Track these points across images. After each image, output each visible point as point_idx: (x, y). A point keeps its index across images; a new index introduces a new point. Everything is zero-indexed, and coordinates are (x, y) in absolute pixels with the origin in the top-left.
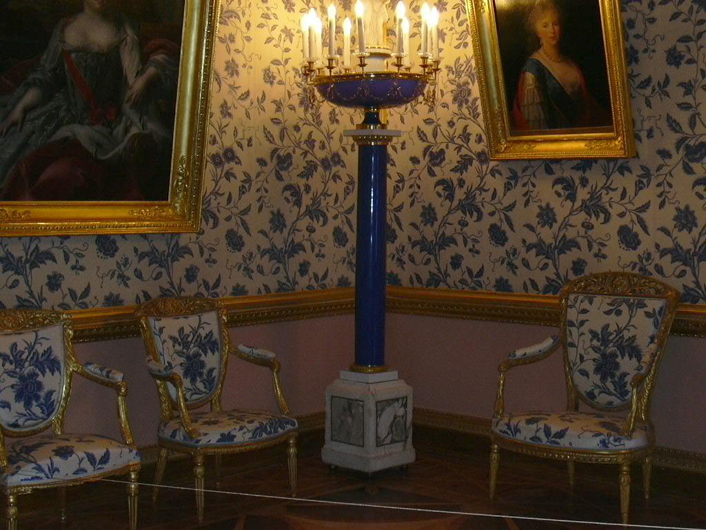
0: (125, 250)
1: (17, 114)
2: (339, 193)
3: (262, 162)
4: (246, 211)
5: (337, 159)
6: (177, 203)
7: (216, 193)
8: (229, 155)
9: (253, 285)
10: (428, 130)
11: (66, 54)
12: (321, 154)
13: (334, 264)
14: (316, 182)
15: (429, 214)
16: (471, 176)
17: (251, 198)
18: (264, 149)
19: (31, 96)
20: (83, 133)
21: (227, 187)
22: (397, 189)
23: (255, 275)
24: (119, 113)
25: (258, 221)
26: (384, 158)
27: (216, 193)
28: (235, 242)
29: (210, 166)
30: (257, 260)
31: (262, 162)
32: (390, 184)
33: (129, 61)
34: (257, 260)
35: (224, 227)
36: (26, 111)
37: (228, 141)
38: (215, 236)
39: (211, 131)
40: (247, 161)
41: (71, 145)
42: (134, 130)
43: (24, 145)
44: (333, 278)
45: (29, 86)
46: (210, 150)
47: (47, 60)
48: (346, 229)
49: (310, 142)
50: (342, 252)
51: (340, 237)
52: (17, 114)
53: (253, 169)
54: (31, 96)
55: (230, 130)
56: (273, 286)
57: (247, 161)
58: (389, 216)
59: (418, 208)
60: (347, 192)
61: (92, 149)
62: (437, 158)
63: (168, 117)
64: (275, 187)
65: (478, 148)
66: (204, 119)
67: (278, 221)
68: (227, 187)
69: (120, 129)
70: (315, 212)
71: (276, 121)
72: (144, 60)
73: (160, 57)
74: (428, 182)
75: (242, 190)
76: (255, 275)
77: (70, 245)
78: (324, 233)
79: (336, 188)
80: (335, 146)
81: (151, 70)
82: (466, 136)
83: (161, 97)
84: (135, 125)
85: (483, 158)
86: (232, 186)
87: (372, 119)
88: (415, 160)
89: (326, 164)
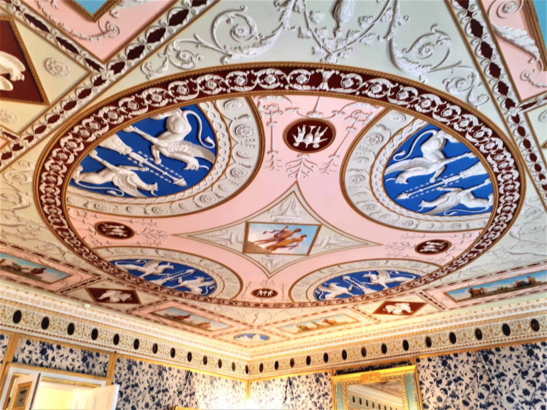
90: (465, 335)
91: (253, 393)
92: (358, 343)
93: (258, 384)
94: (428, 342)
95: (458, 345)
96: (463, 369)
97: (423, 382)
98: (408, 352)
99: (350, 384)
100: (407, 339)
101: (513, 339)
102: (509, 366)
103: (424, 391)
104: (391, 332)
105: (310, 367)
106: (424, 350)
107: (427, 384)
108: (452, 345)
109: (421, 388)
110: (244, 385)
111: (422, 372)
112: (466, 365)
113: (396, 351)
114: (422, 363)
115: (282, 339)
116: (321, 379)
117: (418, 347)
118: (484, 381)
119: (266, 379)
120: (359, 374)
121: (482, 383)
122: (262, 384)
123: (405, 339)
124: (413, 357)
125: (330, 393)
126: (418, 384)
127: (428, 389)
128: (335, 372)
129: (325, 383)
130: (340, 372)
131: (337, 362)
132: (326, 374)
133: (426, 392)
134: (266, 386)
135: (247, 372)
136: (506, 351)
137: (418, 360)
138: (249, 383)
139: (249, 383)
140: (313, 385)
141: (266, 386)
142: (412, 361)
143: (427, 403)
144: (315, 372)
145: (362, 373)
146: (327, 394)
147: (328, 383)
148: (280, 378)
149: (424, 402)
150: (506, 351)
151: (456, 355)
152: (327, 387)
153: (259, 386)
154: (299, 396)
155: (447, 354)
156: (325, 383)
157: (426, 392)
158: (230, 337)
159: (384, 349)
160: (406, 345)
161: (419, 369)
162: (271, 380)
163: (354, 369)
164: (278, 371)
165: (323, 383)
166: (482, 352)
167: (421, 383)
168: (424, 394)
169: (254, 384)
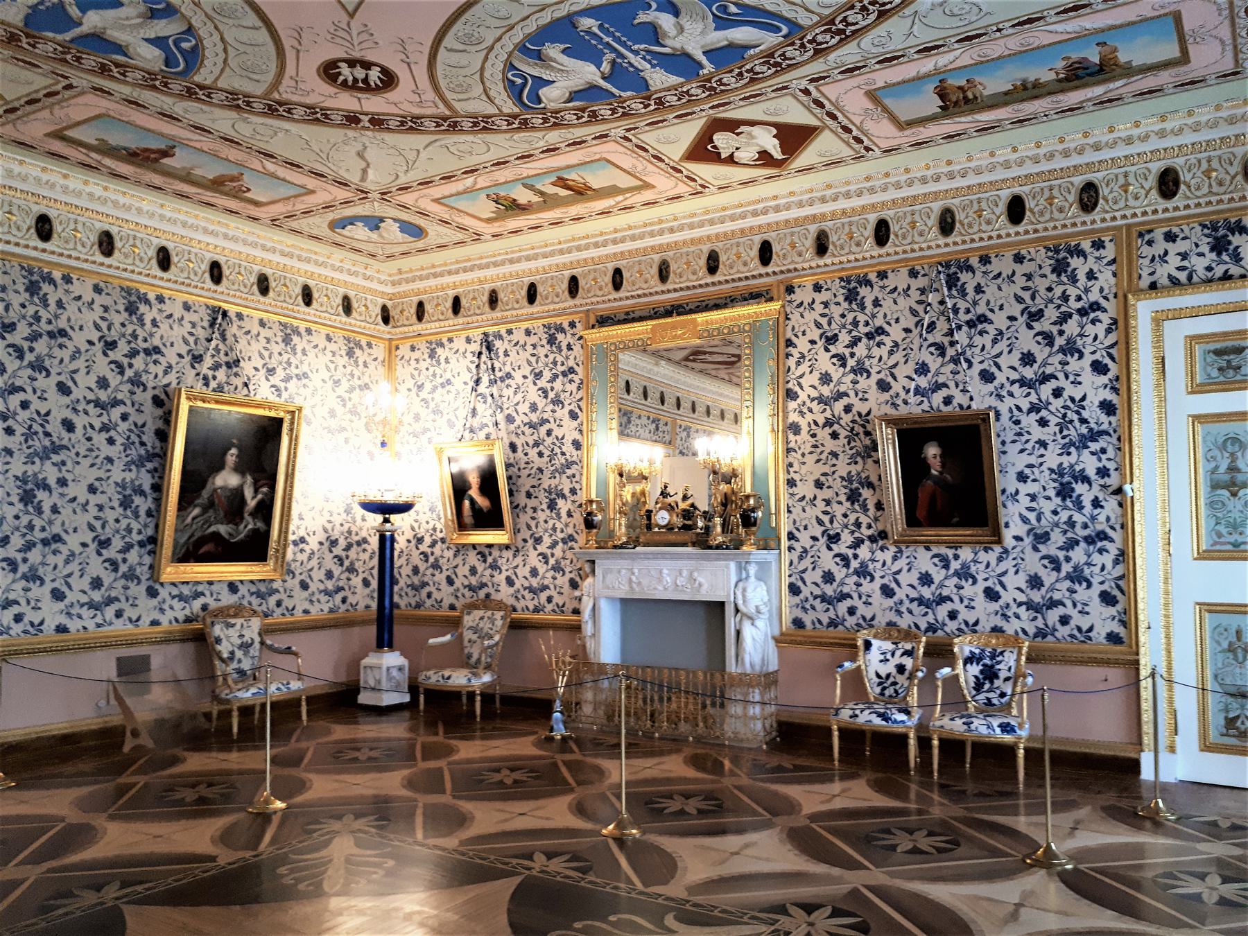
0: (243, 590)
1: (189, 520)
2: (367, 561)
3: (321, 544)
4: (311, 570)
5: (365, 541)
6: (271, 562)
7: (294, 561)
8: (302, 540)
9: (314, 610)
10: (416, 525)
11: (215, 490)
12: (357, 538)
13: (363, 598)
14: (352, 553)
15: (416, 570)
16: (437, 550)
17: (314, 562)
18: (321, 536)
19: (196, 511)
20: (223, 529)
21: (300, 557)
22: (400, 557)
23: (316, 603)
24: (242, 518)
25: (318, 575)
26: (393, 539)
27: (294, 561)
28: (304, 586)
29: (291, 546)
30: (317, 596)
31: (321, 544)
32: (396, 553)
33: (248, 492)
34: (317, 596)
35: (298, 578)
36: (194, 519)
37: (302, 533)
38: (294, 583)
39: (292, 528)
40: (313, 543)
41: (216, 535)
42: (250, 527)
43: (192, 535)
44: (361, 607)
45: (195, 506)
46: (291, 538)
47: (205, 494)
48: (370, 578)
49: (349, 532)
50: (367, 591)
51: (366, 583)
52: (189, 520)
53: (315, 547)
54: (196, 511)
55: (303, 528)
56: (326, 610)
57: (313, 543)
58: (396, 571)
59: (410, 567)
60: (371, 558)
61: (227, 537)
62: (420, 540)
63: (268, 520)
64: (329, 556)
65: (441, 535)
66: (288, 521)
67: (329, 575)
68: (300, 557)
69: (242, 527)
70: (351, 570)
71: (329, 522)
72: (256, 491)
73: (265, 489)
74: (415, 553)
75: (310, 559)
76: (316, 603)
77: (214, 588)
78: (357, 581)
79: (366, 556)
80: (364, 534)
81: (260, 496)
82: (434, 529)
83: (264, 510)
84: (249, 524)
85: (443, 540)
86: (304, 557)
87: (386, 521)
88: (409, 541)
89: (359, 544)
90: (913, 224)
91: (403, 371)
92: (653, 248)
93: (413, 348)
94: (821, 247)
95: (891, 250)
96: (895, 307)
97: (794, 340)
98: (769, 269)
99: (626, 348)
100: (771, 236)
101: (1027, 232)
102: (1001, 301)
103: (792, 362)
104: (733, 218)
105: (535, 309)
106: (806, 265)
107: (802, 345)
108: (877, 251)
109: (788, 355)
110: (379, 351)
111: (795, 317)
112: (901, 300)
113: (741, 266)
114: (798, 296)
115: (460, 236)
116: (560, 337)
117: (795, 256)
118: (937, 337)
119: (433, 338)
120: (647, 325)
121: (931, 339)
122: (422, 345)
123: (766, 237)
124: (781, 282)
125: (579, 370)
126: (782, 344)
127: (803, 357)
128: (592, 321)
129: (569, 348)
130: (603, 321)
131: (599, 297)
132: (572, 325)
133: (798, 363)
134: (432, 354)
135: (386, 320)
136: (1003, 265)
137: (790, 290)
138: (392, 348)
139: (392, 348)
140: (541, 352)
141: (432, 354)
142: (774, 293)
143: (797, 389)
144: (546, 321)
145: (654, 322)
146: (572, 370)
147: (577, 348)
148: (464, 334)
149: (790, 385)
150: (1003, 265)
151: (882, 275)
152: (572, 354)
153: (417, 354)
154: (509, 376)
155: (861, 272)
156: (569, 348)
157: (798, 363)
158: (318, 223)
159: (713, 264)
160: (766, 253)
161: (788, 310)
162: (445, 340)
163: (637, 314)
164: (460, 320)
165: (564, 347)
166: (947, 265)
167: (789, 343)
168: (793, 367)
169: (404, 350)
